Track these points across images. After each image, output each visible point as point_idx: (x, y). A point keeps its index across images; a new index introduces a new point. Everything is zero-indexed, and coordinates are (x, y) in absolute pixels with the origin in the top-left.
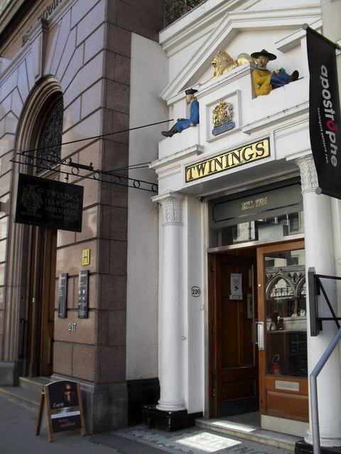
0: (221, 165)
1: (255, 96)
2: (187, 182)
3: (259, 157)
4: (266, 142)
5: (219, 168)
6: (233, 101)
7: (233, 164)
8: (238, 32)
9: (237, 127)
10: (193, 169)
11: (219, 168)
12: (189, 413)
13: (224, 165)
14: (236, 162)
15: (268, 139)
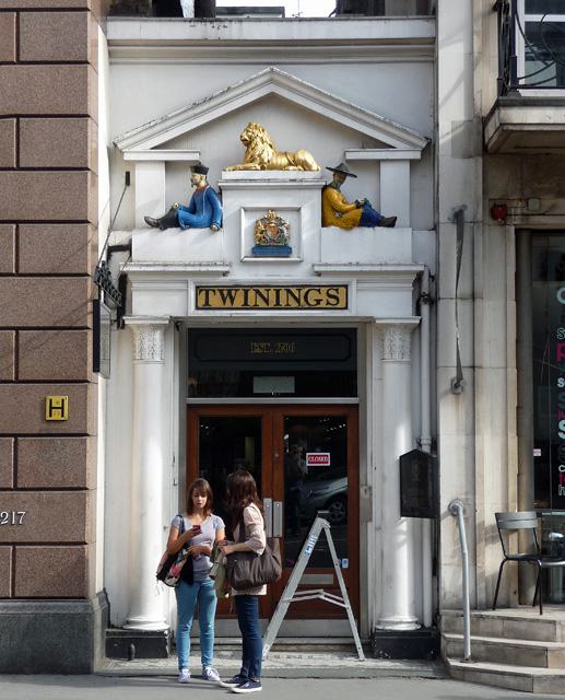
0: (267, 301)
1: (324, 224)
4: (342, 290)
5: (261, 303)
6: (287, 218)
8: (271, 101)
12: (175, 629)
14: (293, 303)
15: (346, 286)
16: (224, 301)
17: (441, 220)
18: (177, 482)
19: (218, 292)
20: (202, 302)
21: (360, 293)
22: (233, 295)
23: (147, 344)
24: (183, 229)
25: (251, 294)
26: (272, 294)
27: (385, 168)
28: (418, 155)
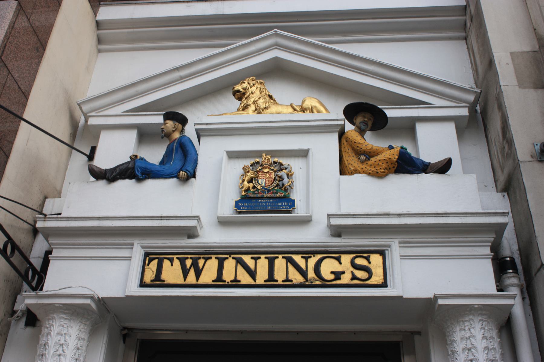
0: (252, 274)
2: (143, 285)
3: (356, 282)
4: (376, 259)
5: (246, 279)
7: (287, 280)
9: (300, 211)
10: (166, 263)
13: (262, 275)
14: (297, 277)
16: (185, 273)
19: (177, 262)
20: (149, 276)
22: (201, 266)
26: (263, 266)
27: (421, 129)
28: (464, 112)
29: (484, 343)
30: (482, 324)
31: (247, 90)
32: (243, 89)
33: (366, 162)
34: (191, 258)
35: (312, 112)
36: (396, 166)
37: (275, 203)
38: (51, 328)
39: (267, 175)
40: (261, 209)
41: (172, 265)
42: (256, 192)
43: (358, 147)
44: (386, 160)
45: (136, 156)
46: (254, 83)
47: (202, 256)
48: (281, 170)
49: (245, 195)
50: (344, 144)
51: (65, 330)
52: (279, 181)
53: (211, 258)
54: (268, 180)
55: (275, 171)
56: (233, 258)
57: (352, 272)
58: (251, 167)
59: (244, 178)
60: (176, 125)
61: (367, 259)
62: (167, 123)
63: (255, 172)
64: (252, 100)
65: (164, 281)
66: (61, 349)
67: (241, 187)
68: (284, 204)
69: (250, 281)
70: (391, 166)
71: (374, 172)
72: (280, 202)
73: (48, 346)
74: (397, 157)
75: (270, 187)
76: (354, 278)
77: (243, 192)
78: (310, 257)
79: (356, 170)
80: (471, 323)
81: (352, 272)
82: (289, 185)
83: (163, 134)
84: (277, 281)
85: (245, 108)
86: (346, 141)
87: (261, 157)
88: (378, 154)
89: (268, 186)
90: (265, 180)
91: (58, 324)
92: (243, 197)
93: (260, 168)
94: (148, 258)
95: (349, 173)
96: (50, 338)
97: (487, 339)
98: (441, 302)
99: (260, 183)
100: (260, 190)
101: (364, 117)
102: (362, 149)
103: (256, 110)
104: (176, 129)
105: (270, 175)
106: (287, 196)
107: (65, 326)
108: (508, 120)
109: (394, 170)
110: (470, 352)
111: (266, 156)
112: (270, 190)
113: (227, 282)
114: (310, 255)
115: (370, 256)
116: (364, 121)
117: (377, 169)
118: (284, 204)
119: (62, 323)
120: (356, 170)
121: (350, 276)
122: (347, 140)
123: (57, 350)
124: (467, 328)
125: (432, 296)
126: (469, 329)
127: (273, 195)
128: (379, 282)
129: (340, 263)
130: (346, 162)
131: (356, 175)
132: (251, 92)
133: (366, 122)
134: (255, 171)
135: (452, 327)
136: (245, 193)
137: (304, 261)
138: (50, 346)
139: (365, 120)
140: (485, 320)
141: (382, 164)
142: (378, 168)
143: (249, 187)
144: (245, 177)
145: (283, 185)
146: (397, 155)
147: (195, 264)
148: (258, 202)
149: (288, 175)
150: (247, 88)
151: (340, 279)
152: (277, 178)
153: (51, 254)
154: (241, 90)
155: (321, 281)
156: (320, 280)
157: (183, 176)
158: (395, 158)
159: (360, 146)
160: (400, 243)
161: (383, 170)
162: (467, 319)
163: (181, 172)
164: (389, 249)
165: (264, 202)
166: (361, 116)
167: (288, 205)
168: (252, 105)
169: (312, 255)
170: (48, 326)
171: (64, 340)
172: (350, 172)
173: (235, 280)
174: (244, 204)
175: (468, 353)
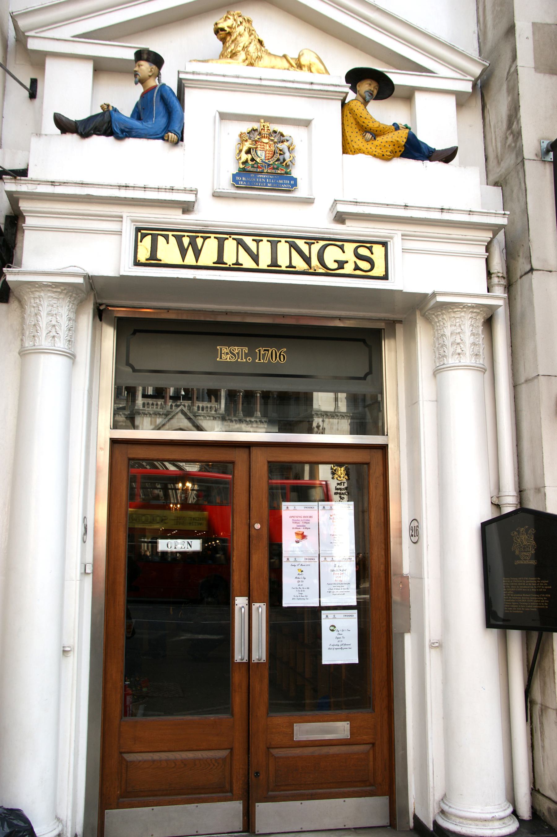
0: (255, 258)
2: (137, 263)
3: (358, 272)
4: (378, 250)
5: (247, 261)
7: (291, 266)
9: (301, 192)
10: (161, 240)
11: (247, 261)
13: (265, 261)
15: (385, 244)
16: (183, 252)
17: (526, 156)
18: (89, 570)
19: (172, 240)
20: (144, 254)
21: (407, 255)
23: (44, 321)
24: (119, 138)
25: (230, 245)
28: (467, 87)
29: (472, 339)
30: (472, 322)
31: (233, 29)
32: (228, 27)
33: (371, 142)
34: (188, 236)
35: (311, 72)
36: (403, 150)
37: (276, 181)
38: (38, 307)
39: (266, 146)
40: (261, 186)
41: (168, 243)
42: (255, 166)
43: (364, 122)
44: (394, 142)
45: (108, 106)
46: (241, 21)
47: (200, 235)
48: (283, 142)
49: (244, 168)
50: (346, 116)
51: (55, 310)
52: (280, 154)
53: (210, 237)
54: (268, 152)
55: (275, 143)
56: (233, 239)
57: (355, 262)
58: (248, 135)
59: (241, 148)
60: (152, 68)
61: (370, 249)
62: (142, 65)
63: (253, 141)
64: (242, 45)
65: (160, 260)
66: (54, 330)
67: (238, 158)
68: (286, 182)
69: (253, 265)
70: (397, 150)
71: (380, 155)
72: (281, 180)
73: (40, 327)
74: (405, 140)
75: (270, 162)
76: (357, 268)
77: (241, 164)
78: (314, 243)
79: (360, 150)
80: (462, 320)
81: (355, 262)
82: (291, 161)
83: (137, 79)
84: (280, 267)
85: (233, 55)
86: (350, 113)
87: (259, 121)
88: (384, 134)
89: (268, 159)
90: (264, 152)
91: (46, 304)
92: (242, 170)
93: (258, 137)
94: (139, 234)
95: (351, 151)
96: (40, 318)
97: (474, 336)
98: (440, 299)
99: (259, 155)
100: (259, 163)
101: (370, 85)
102: (368, 125)
103: (247, 59)
104: (152, 74)
105: (270, 147)
106: (289, 173)
107: (55, 306)
108: (519, 110)
109: (400, 154)
110: (458, 346)
111: (264, 122)
112: (271, 164)
113: (228, 264)
114: (313, 241)
115: (372, 247)
116: (370, 91)
117: (382, 151)
118: (286, 182)
119: (51, 303)
120: (360, 150)
121: (353, 266)
122: (352, 112)
123: (50, 332)
124: (458, 324)
125: (429, 291)
126: (460, 326)
127: (273, 171)
128: (381, 275)
129: (344, 252)
130: (348, 138)
131: (360, 156)
132: (238, 33)
133: (372, 92)
134: (253, 140)
135: (443, 322)
136: (243, 165)
137: (307, 246)
138: (41, 327)
139: (370, 90)
140: (474, 317)
141: (388, 146)
142: (385, 151)
143: (247, 159)
144: (243, 146)
145: (284, 160)
146: (405, 138)
147: (193, 243)
148: (257, 178)
149: (289, 148)
150: (234, 26)
151: (343, 268)
152: (277, 151)
153: (24, 223)
154: (226, 29)
155: (325, 269)
156: (324, 268)
157: (173, 140)
158: (403, 141)
159: (365, 120)
160: (402, 235)
161: (389, 154)
162: (459, 316)
163: (170, 134)
164: (391, 241)
165: (264, 178)
166: (367, 84)
167: (290, 184)
168: (242, 52)
169: (315, 242)
170: (35, 305)
171: (55, 321)
172: (353, 150)
173: (237, 263)
174: (242, 179)
175: (456, 347)
